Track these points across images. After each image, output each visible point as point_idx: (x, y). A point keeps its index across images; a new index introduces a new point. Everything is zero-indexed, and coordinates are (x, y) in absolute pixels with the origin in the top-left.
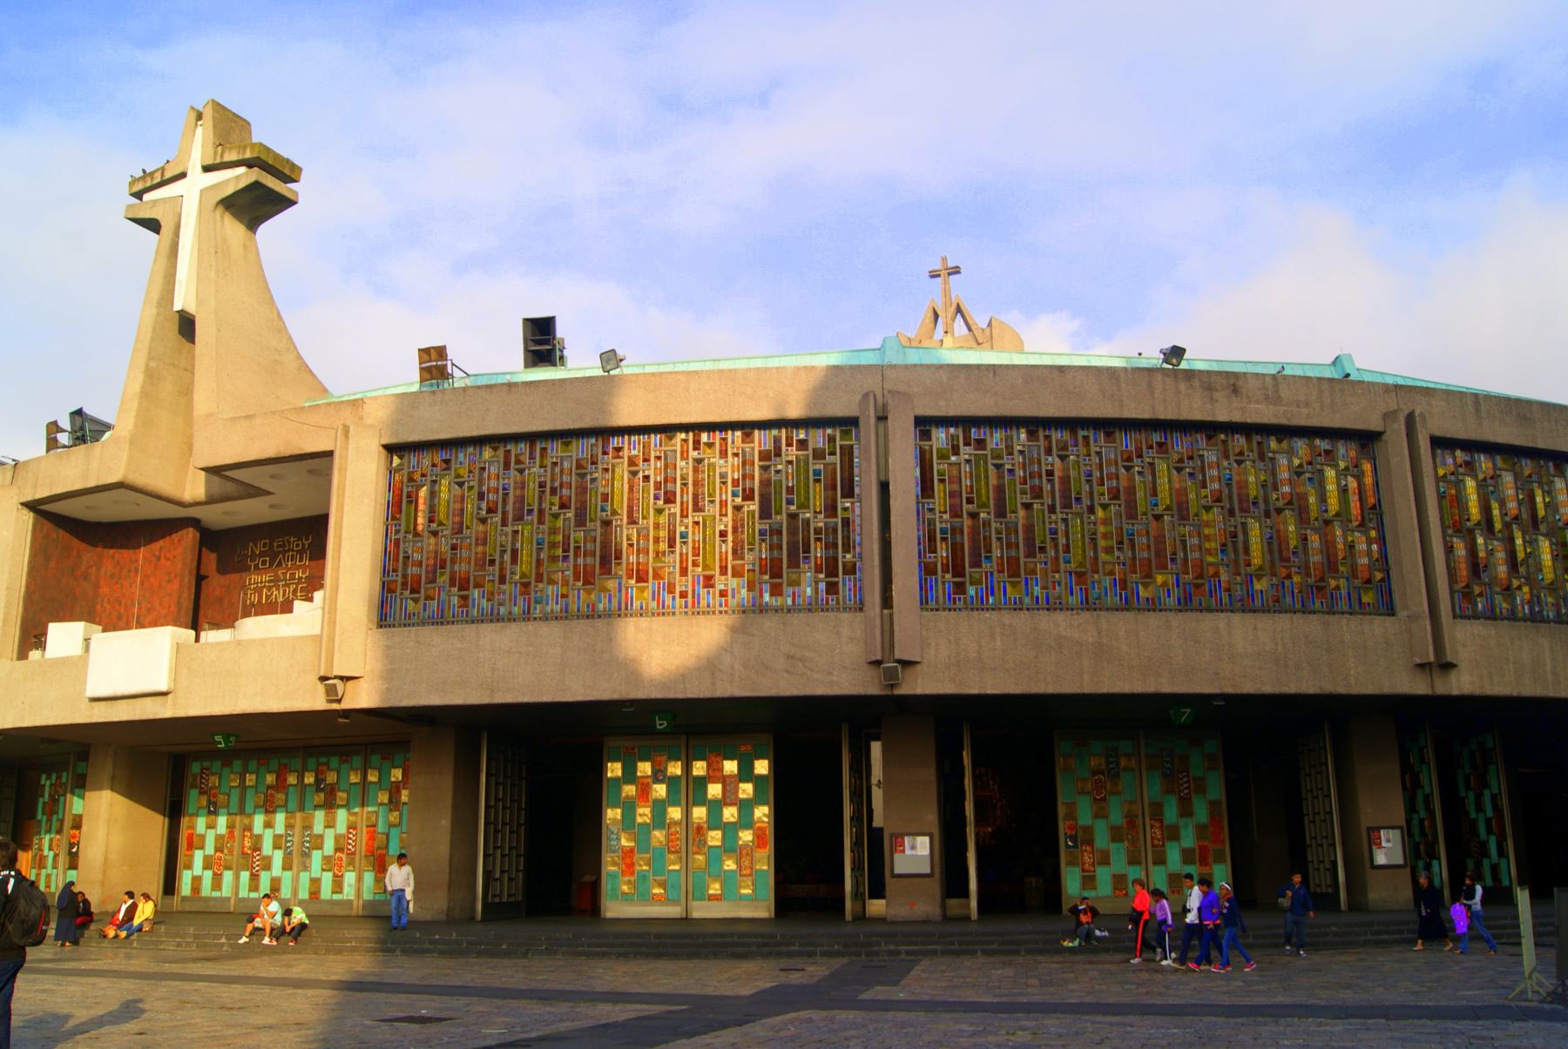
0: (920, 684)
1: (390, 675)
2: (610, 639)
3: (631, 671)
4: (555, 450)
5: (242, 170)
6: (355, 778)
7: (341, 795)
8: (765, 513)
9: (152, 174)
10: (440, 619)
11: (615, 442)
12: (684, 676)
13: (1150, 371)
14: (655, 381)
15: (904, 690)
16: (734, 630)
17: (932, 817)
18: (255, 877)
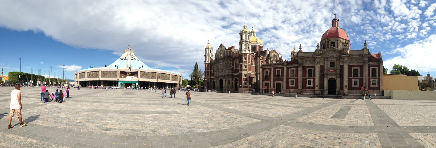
0: (158, 82)
10: (142, 78)
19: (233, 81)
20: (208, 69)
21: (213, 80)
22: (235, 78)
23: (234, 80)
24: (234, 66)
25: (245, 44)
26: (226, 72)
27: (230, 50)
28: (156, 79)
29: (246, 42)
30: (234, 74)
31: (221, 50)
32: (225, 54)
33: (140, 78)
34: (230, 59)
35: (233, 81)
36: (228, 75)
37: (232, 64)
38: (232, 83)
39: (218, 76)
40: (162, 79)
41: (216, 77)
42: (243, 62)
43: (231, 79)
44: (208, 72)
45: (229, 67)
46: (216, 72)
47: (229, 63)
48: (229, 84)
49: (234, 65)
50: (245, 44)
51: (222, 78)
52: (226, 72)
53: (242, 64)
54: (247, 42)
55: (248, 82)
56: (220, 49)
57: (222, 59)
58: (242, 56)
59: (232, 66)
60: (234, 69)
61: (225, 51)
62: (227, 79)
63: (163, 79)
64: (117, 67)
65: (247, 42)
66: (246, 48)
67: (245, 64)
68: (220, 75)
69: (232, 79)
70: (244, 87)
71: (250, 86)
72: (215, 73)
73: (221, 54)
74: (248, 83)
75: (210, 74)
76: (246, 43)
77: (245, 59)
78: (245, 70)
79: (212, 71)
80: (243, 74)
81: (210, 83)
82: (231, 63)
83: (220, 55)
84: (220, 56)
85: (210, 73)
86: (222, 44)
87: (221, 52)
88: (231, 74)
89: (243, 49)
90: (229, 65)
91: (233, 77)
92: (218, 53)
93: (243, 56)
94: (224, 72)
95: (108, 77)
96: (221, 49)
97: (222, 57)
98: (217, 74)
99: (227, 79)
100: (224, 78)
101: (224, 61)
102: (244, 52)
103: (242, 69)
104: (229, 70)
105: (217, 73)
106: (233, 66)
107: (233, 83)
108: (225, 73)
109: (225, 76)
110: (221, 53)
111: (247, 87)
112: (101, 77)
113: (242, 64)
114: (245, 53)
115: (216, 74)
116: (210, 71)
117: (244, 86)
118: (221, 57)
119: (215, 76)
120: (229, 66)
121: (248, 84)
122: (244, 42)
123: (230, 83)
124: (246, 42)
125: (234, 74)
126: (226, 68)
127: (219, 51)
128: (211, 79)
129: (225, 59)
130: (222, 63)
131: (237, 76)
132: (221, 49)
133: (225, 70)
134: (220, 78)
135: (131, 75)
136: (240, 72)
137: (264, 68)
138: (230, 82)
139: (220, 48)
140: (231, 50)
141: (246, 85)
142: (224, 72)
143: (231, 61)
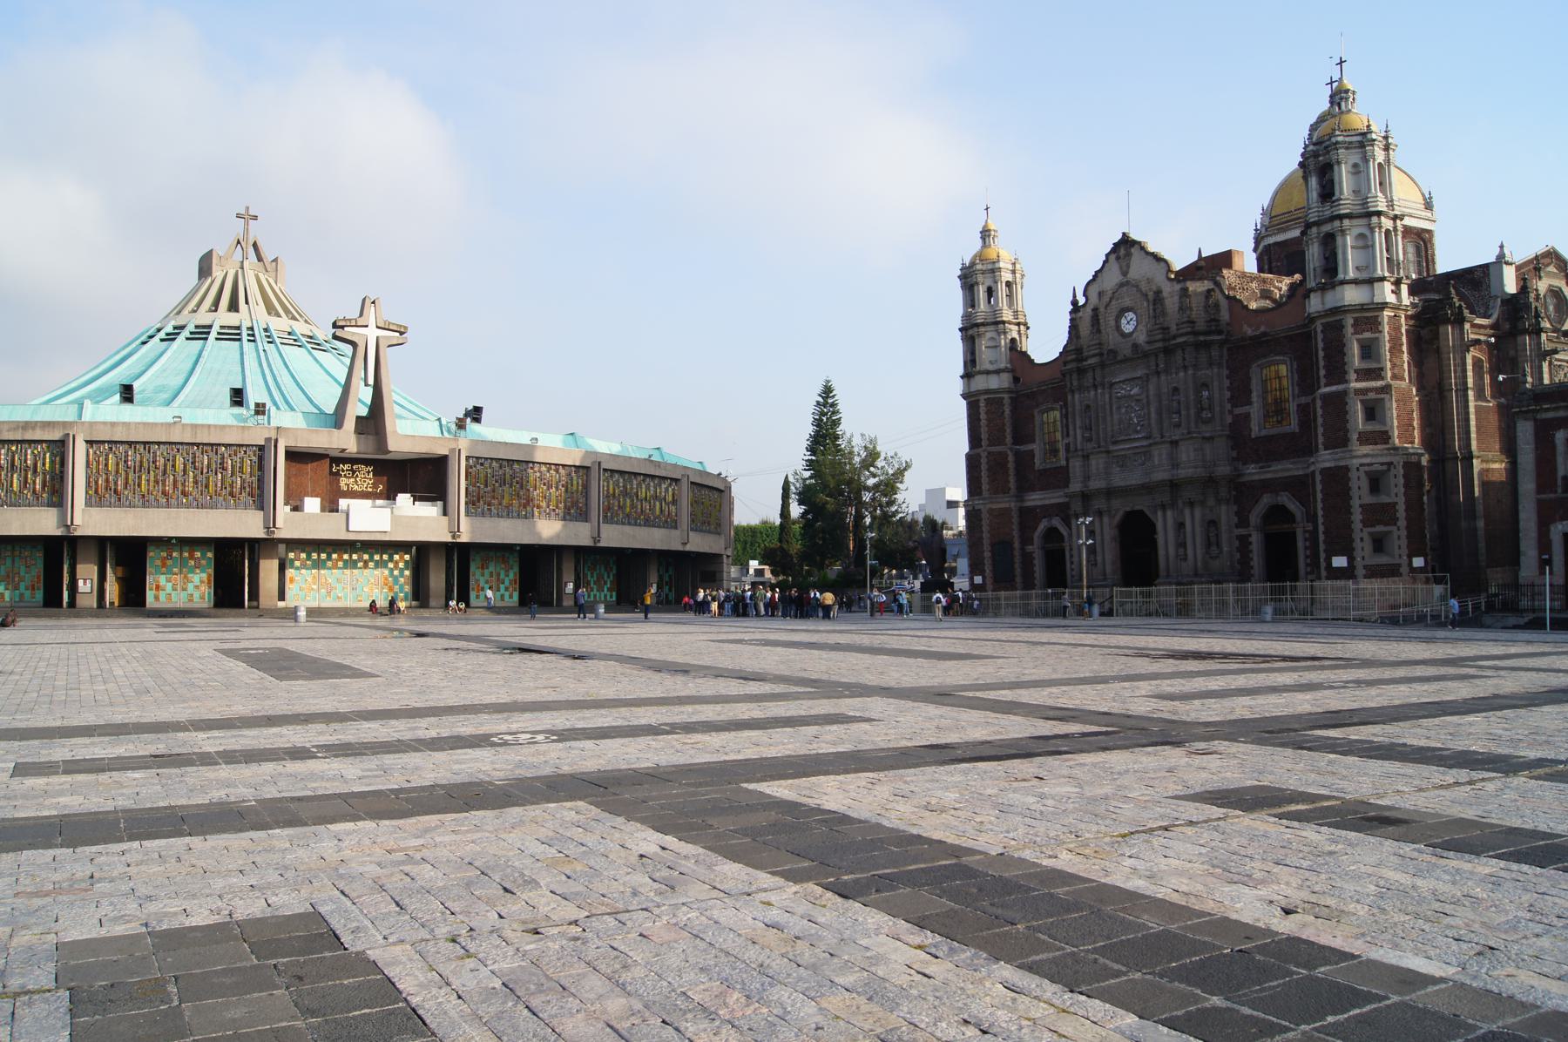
0: (602, 544)
1: (473, 532)
2: (534, 526)
3: (539, 535)
4: (516, 466)
5: (398, 334)
6: (377, 557)
7: (371, 564)
8: (566, 491)
9: (350, 320)
10: (483, 515)
11: (531, 465)
12: (552, 538)
13: (645, 459)
14: (546, 448)
15: (598, 545)
16: (564, 526)
17: (573, 578)
18: (329, 593)
19: (1243, 522)
20: (996, 439)
21: (1043, 526)
22: (1266, 500)
23: (1255, 518)
24: (1255, 410)
25: (1361, 236)
26: (1187, 453)
27: (1207, 285)
28: (587, 525)
29: (1370, 215)
30: (1252, 472)
31: (1122, 285)
32: (1164, 313)
33: (467, 514)
34: (1215, 353)
35: (1243, 522)
36: (1210, 482)
37: (1228, 394)
38: (1237, 543)
39: (1110, 493)
40: (629, 524)
41: (1086, 497)
42: (1353, 376)
43: (1226, 515)
44: (998, 464)
45: (1205, 414)
46: (1086, 457)
47: (1205, 385)
48: (1214, 548)
49: (1249, 403)
50: (1356, 231)
51: (1142, 504)
52: (1187, 453)
53: (1345, 393)
54: (1375, 219)
55: (1404, 533)
56: (1113, 278)
57: (1139, 354)
58: (1339, 326)
59: (1228, 406)
60: (1255, 430)
61: (1170, 290)
62: (1198, 512)
63: (636, 525)
64: (260, 409)
65: (1379, 214)
66: (1370, 264)
67: (1372, 395)
68: (1120, 479)
69: (1235, 508)
70: (1374, 572)
71: (1418, 562)
72: (1076, 465)
73: (1130, 315)
74: (1404, 542)
75: (1012, 479)
76: (1363, 221)
77: (1369, 350)
78: (1365, 439)
79: (1031, 454)
80: (1353, 475)
81: (1017, 545)
82: (1227, 383)
83: (1113, 323)
84: (1118, 327)
85: (1011, 465)
86: (1134, 236)
87: (1127, 302)
88: (1223, 470)
89: (1341, 276)
90: (1205, 403)
91: (1243, 493)
92: (1095, 310)
93: (1349, 330)
94: (1160, 454)
95: (167, 500)
96: (1125, 274)
97: (1141, 338)
98: (1096, 473)
99: (1198, 512)
100: (1163, 507)
101: (1158, 373)
102: (1352, 296)
103: (1348, 431)
104: (1211, 439)
105: (1097, 463)
106: (1238, 411)
107: (1244, 541)
108: (1175, 465)
109: (1174, 486)
110: (1123, 311)
111: (1391, 571)
112: (96, 498)
113: (1345, 393)
114: (1362, 308)
115: (1087, 478)
116: (1017, 454)
117: (1368, 562)
118: (1123, 335)
119: (1075, 486)
120: (1211, 408)
121: (1405, 551)
122: (1341, 217)
123: (1218, 545)
124: (1370, 215)
125: (1252, 472)
126: (1178, 425)
127: (1100, 294)
128: (1029, 517)
129: (1168, 351)
130: (1135, 390)
131: (1299, 487)
132: (1125, 274)
133: (1174, 443)
134: (1121, 507)
135: (375, 486)
136: (1326, 459)
137: (1551, 415)
138: (1224, 537)
139: (1114, 266)
140: (1218, 284)
141: (1383, 560)
142: (1160, 454)
143: (1225, 372)
